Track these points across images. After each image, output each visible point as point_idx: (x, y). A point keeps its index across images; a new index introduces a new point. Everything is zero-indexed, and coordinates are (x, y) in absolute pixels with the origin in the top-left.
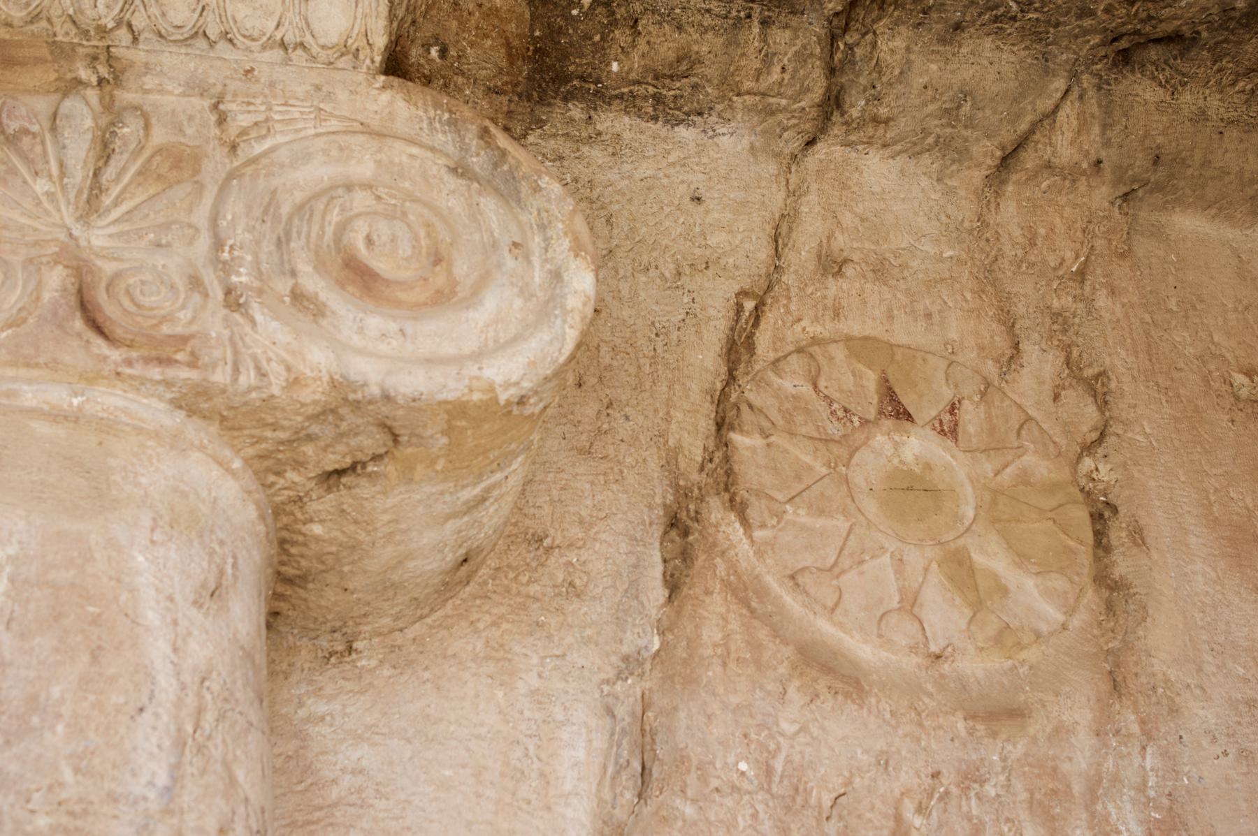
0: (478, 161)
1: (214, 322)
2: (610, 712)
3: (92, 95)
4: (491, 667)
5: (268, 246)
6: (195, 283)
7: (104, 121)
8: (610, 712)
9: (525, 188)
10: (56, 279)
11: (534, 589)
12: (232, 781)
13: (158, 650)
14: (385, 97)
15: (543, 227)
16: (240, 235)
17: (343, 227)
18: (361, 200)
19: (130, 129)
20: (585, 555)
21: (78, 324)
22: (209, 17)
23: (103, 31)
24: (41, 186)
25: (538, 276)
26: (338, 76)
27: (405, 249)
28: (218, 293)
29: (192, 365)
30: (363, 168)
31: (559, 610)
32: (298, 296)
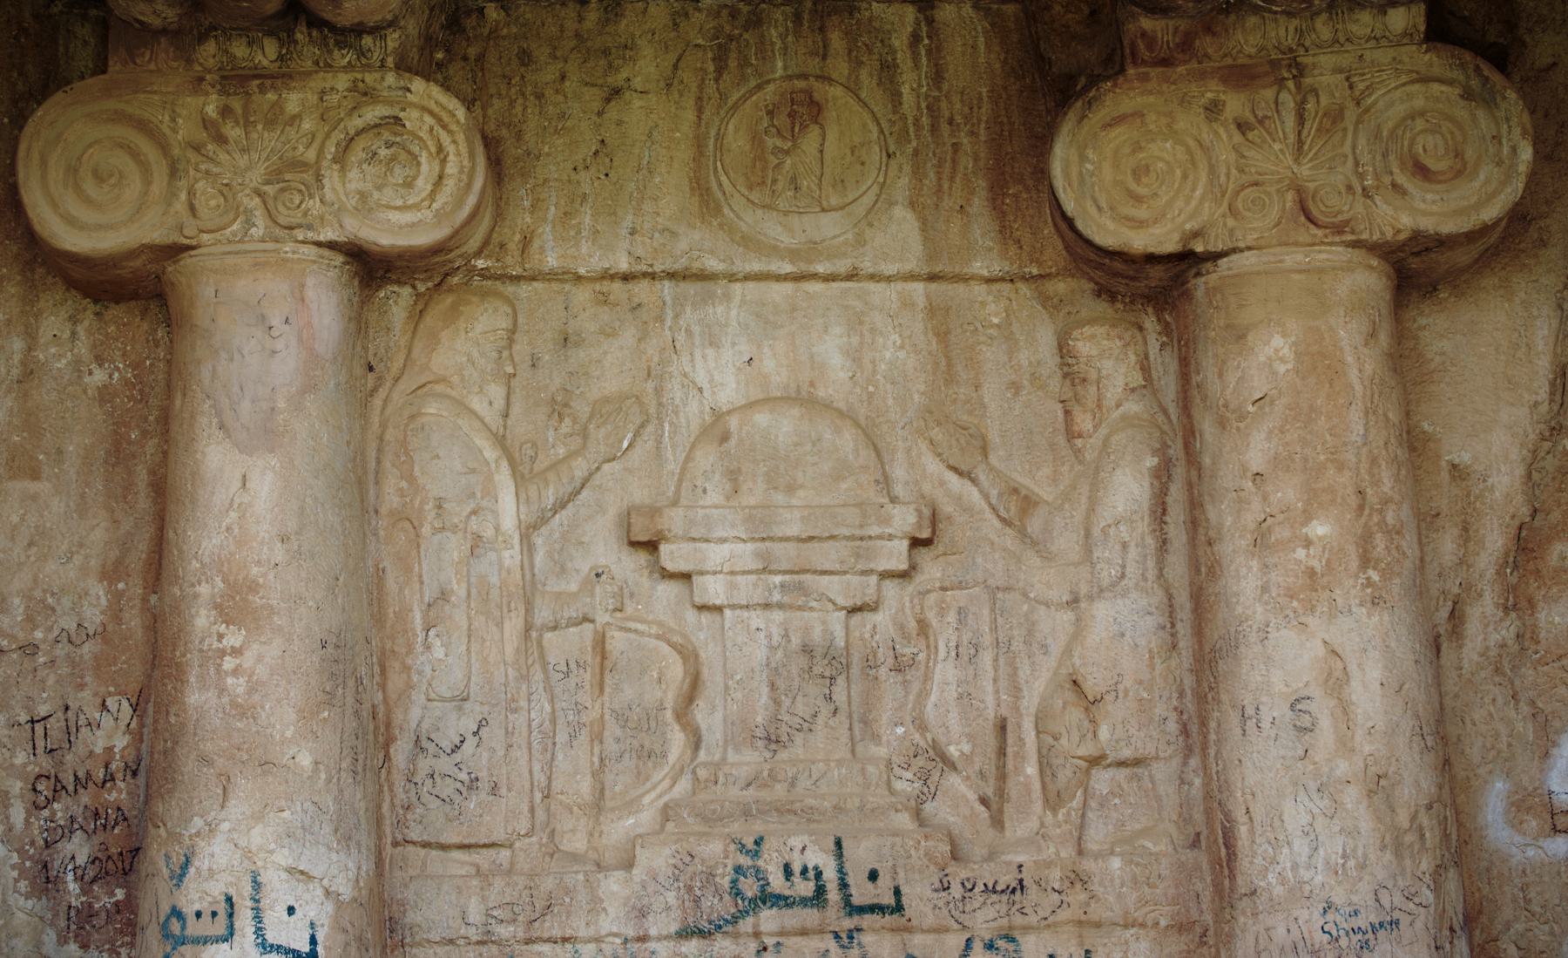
0: (1475, 83)
1: (1359, 208)
2: (1560, 307)
3: (1291, 84)
4: (1502, 292)
5: (1379, 157)
6: (1350, 188)
7: (1298, 98)
8: (1560, 307)
9: (1499, 99)
10: (1290, 196)
11: (1522, 246)
12: (1387, 419)
13: (1353, 374)
14: (1427, 57)
15: (1508, 120)
16: (1365, 158)
17: (1412, 142)
18: (1420, 124)
19: (1310, 106)
20: (1548, 221)
21: (1303, 218)
22: (1340, 34)
23: (1291, 50)
24: (1277, 146)
25: (1506, 150)
26: (1404, 49)
27: (1441, 151)
28: (1359, 190)
29: (1353, 232)
30: (1419, 103)
31: (1536, 256)
32: (1394, 185)
